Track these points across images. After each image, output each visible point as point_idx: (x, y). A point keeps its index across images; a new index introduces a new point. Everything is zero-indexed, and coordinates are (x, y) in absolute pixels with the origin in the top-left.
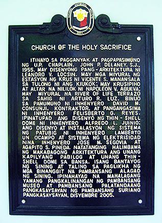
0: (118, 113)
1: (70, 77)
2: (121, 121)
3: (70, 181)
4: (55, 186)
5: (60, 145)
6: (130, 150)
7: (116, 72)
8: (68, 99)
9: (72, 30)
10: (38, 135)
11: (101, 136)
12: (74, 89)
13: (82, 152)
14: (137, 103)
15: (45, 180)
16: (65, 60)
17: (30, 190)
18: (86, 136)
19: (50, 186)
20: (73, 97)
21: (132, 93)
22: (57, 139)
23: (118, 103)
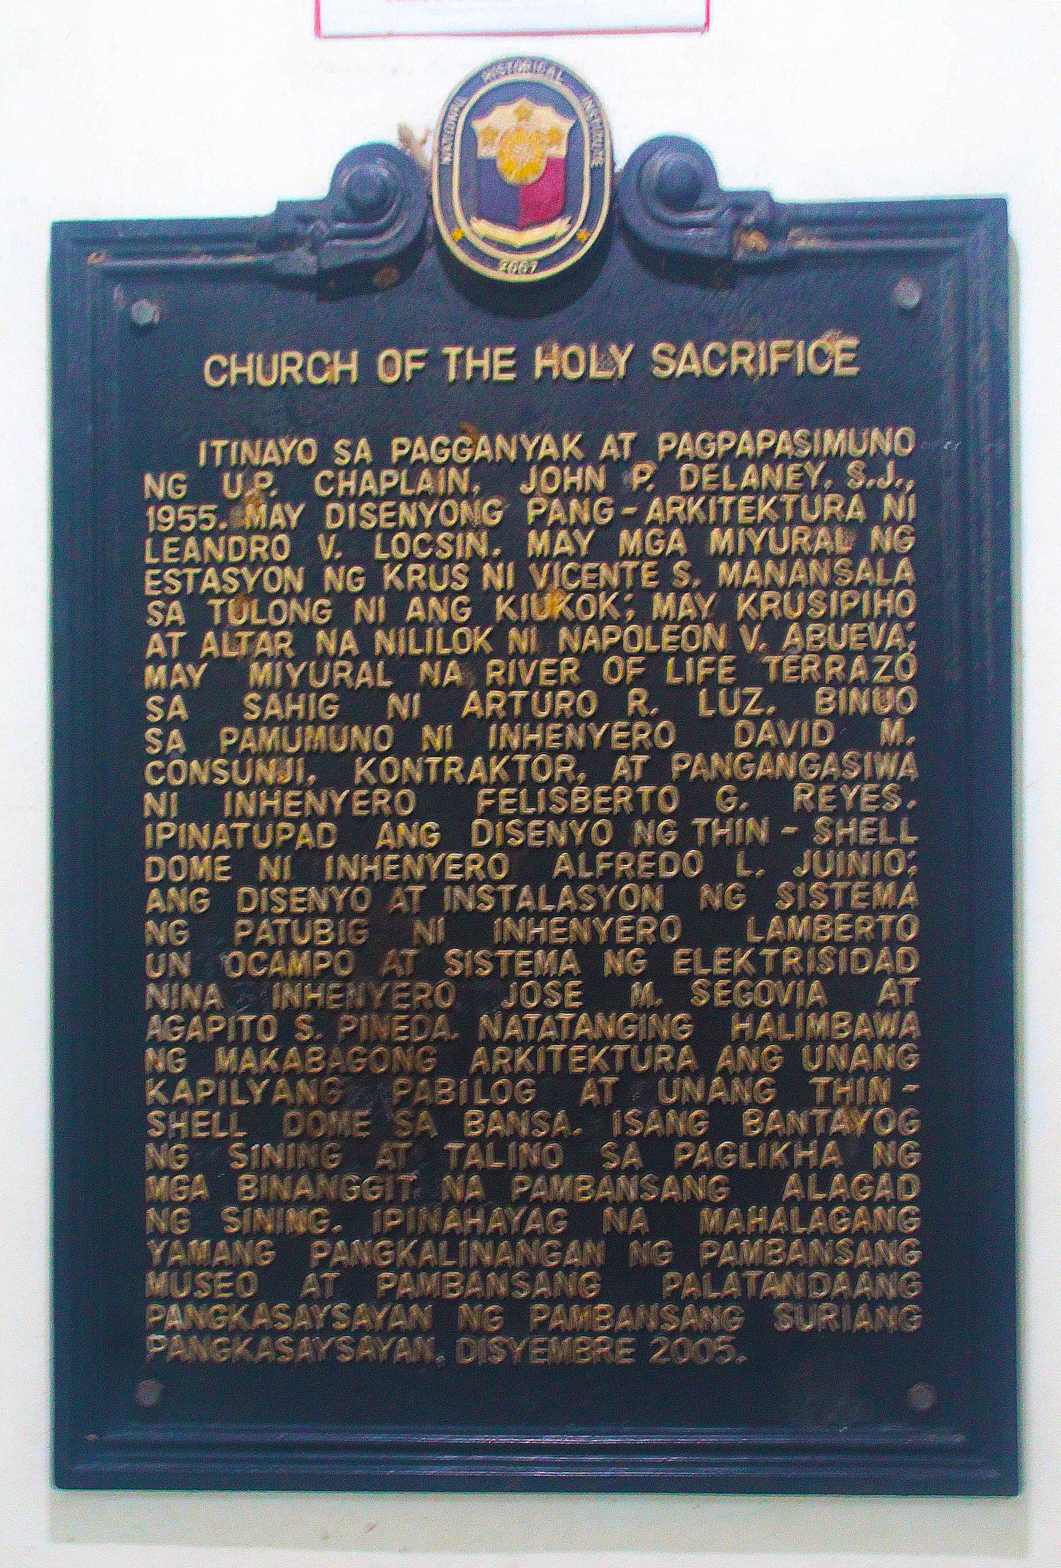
0: (768, 796)
1: (452, 560)
2: (778, 858)
4: (357, 1284)
5: (385, 1008)
6: (852, 1042)
7: (756, 526)
8: (442, 704)
9: (464, 243)
10: (248, 945)
11: (658, 954)
12: (479, 640)
13: (532, 1057)
14: (891, 731)
16: (420, 450)
18: (561, 948)
19: (322, 1283)
20: (473, 695)
23: (766, 733)
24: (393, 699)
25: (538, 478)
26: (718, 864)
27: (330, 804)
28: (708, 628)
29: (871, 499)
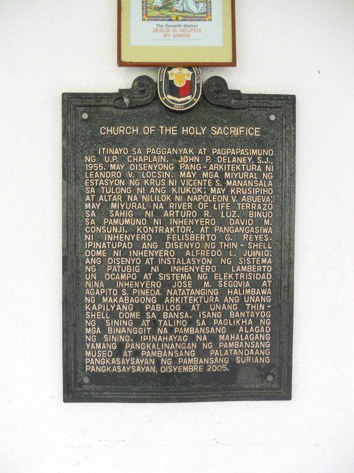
0: (237, 237)
4: (137, 354)
6: (256, 296)
7: (236, 172)
8: (158, 213)
10: (110, 272)
11: (210, 275)
13: (180, 300)
14: (267, 222)
15: (121, 346)
17: (97, 361)
18: (187, 273)
19: (128, 354)
20: (166, 212)
21: (259, 205)
22: (140, 278)
23: (237, 222)
24: (146, 212)
28: (224, 196)
29: (263, 167)
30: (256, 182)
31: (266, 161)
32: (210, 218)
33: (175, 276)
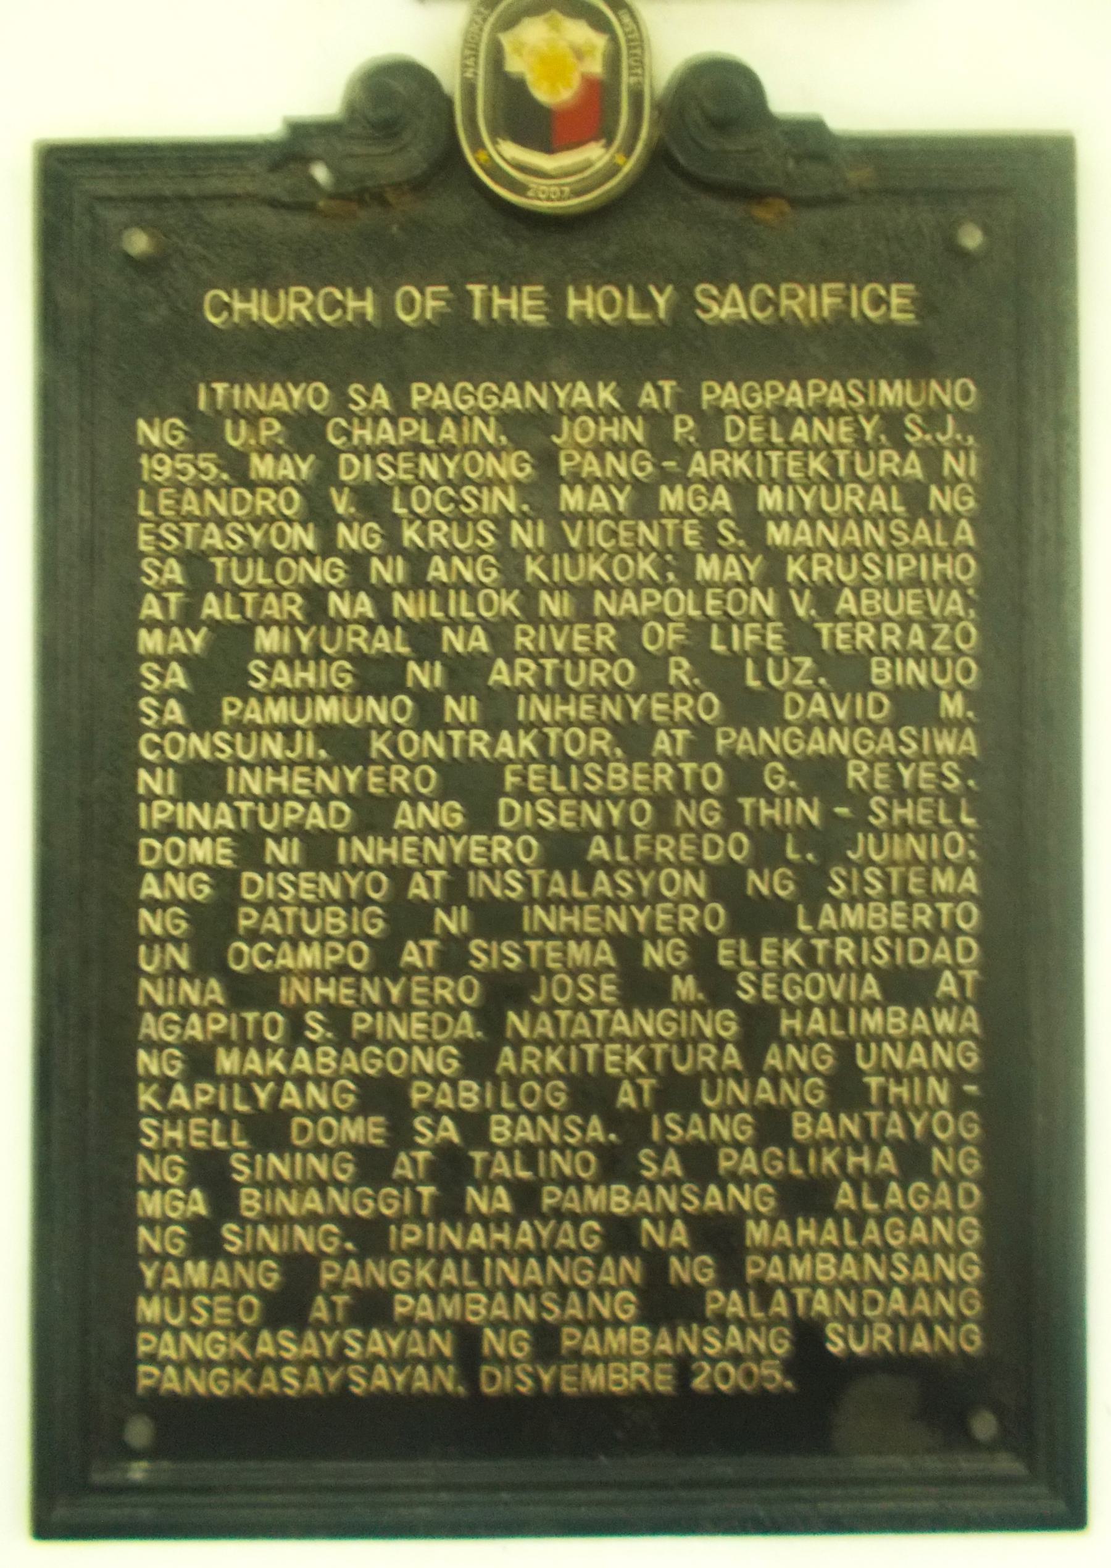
0: (821, 776)
2: (829, 843)
3: (477, 1272)
4: (372, 1308)
5: (405, 1007)
6: (908, 1041)
8: (466, 674)
9: (494, 172)
11: (701, 946)
12: (507, 603)
14: (952, 706)
15: (300, 1270)
16: (442, 398)
17: (189, 1341)
19: (332, 1306)
21: (916, 628)
23: (819, 707)
25: (571, 429)
26: (768, 846)
27: (344, 781)
29: (931, 456)
30: (898, 528)
31: (944, 433)
32: (696, 693)
33: (542, 954)
